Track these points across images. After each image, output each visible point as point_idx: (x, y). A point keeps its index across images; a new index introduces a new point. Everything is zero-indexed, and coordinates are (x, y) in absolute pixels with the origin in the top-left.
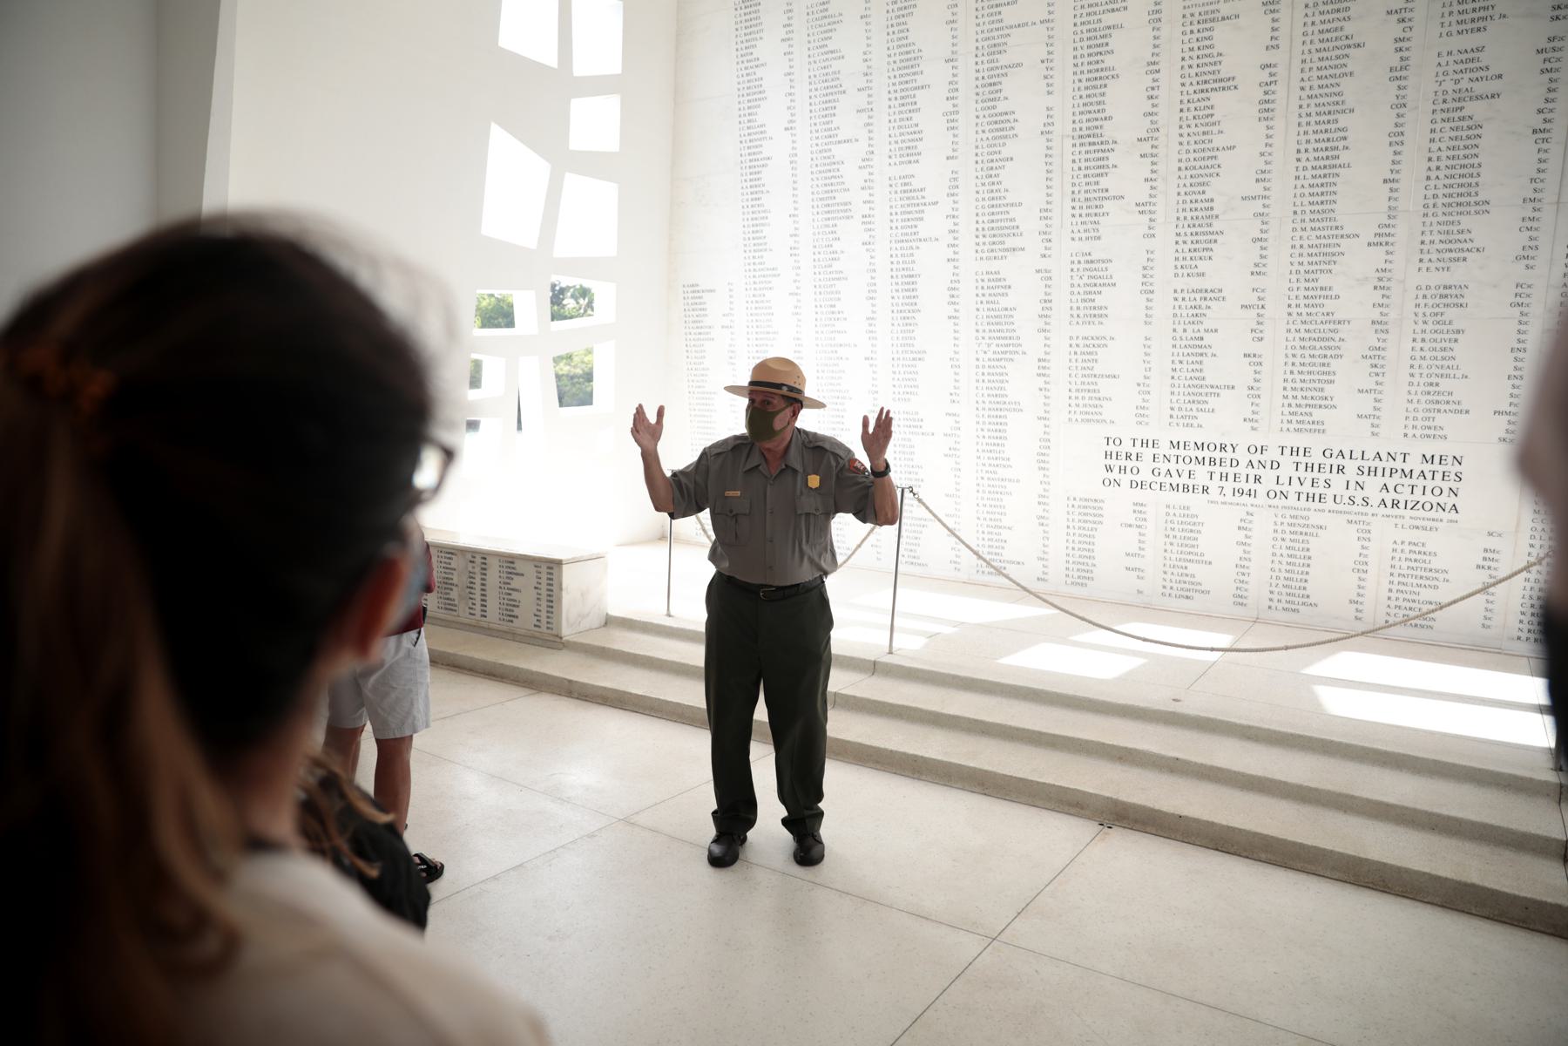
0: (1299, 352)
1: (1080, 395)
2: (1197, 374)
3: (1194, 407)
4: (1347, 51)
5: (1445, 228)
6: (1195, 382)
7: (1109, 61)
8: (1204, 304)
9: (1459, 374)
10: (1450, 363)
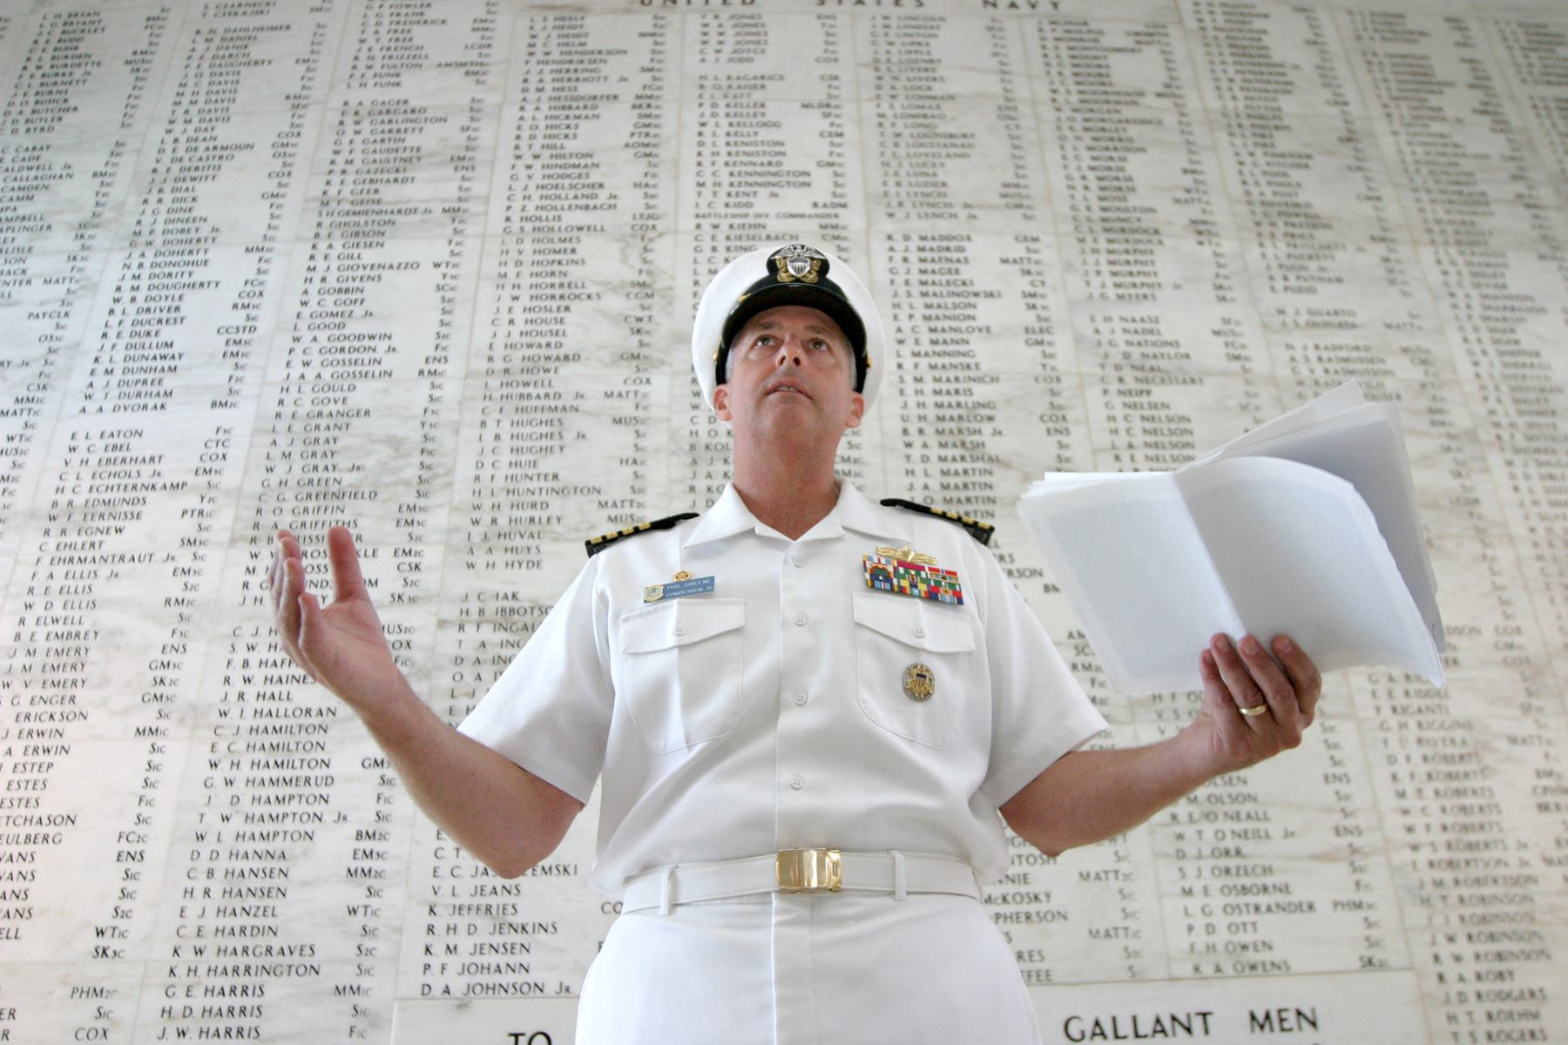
1: (462, 922)
4: (972, 300)
7: (575, 272)
10: (1248, 807)
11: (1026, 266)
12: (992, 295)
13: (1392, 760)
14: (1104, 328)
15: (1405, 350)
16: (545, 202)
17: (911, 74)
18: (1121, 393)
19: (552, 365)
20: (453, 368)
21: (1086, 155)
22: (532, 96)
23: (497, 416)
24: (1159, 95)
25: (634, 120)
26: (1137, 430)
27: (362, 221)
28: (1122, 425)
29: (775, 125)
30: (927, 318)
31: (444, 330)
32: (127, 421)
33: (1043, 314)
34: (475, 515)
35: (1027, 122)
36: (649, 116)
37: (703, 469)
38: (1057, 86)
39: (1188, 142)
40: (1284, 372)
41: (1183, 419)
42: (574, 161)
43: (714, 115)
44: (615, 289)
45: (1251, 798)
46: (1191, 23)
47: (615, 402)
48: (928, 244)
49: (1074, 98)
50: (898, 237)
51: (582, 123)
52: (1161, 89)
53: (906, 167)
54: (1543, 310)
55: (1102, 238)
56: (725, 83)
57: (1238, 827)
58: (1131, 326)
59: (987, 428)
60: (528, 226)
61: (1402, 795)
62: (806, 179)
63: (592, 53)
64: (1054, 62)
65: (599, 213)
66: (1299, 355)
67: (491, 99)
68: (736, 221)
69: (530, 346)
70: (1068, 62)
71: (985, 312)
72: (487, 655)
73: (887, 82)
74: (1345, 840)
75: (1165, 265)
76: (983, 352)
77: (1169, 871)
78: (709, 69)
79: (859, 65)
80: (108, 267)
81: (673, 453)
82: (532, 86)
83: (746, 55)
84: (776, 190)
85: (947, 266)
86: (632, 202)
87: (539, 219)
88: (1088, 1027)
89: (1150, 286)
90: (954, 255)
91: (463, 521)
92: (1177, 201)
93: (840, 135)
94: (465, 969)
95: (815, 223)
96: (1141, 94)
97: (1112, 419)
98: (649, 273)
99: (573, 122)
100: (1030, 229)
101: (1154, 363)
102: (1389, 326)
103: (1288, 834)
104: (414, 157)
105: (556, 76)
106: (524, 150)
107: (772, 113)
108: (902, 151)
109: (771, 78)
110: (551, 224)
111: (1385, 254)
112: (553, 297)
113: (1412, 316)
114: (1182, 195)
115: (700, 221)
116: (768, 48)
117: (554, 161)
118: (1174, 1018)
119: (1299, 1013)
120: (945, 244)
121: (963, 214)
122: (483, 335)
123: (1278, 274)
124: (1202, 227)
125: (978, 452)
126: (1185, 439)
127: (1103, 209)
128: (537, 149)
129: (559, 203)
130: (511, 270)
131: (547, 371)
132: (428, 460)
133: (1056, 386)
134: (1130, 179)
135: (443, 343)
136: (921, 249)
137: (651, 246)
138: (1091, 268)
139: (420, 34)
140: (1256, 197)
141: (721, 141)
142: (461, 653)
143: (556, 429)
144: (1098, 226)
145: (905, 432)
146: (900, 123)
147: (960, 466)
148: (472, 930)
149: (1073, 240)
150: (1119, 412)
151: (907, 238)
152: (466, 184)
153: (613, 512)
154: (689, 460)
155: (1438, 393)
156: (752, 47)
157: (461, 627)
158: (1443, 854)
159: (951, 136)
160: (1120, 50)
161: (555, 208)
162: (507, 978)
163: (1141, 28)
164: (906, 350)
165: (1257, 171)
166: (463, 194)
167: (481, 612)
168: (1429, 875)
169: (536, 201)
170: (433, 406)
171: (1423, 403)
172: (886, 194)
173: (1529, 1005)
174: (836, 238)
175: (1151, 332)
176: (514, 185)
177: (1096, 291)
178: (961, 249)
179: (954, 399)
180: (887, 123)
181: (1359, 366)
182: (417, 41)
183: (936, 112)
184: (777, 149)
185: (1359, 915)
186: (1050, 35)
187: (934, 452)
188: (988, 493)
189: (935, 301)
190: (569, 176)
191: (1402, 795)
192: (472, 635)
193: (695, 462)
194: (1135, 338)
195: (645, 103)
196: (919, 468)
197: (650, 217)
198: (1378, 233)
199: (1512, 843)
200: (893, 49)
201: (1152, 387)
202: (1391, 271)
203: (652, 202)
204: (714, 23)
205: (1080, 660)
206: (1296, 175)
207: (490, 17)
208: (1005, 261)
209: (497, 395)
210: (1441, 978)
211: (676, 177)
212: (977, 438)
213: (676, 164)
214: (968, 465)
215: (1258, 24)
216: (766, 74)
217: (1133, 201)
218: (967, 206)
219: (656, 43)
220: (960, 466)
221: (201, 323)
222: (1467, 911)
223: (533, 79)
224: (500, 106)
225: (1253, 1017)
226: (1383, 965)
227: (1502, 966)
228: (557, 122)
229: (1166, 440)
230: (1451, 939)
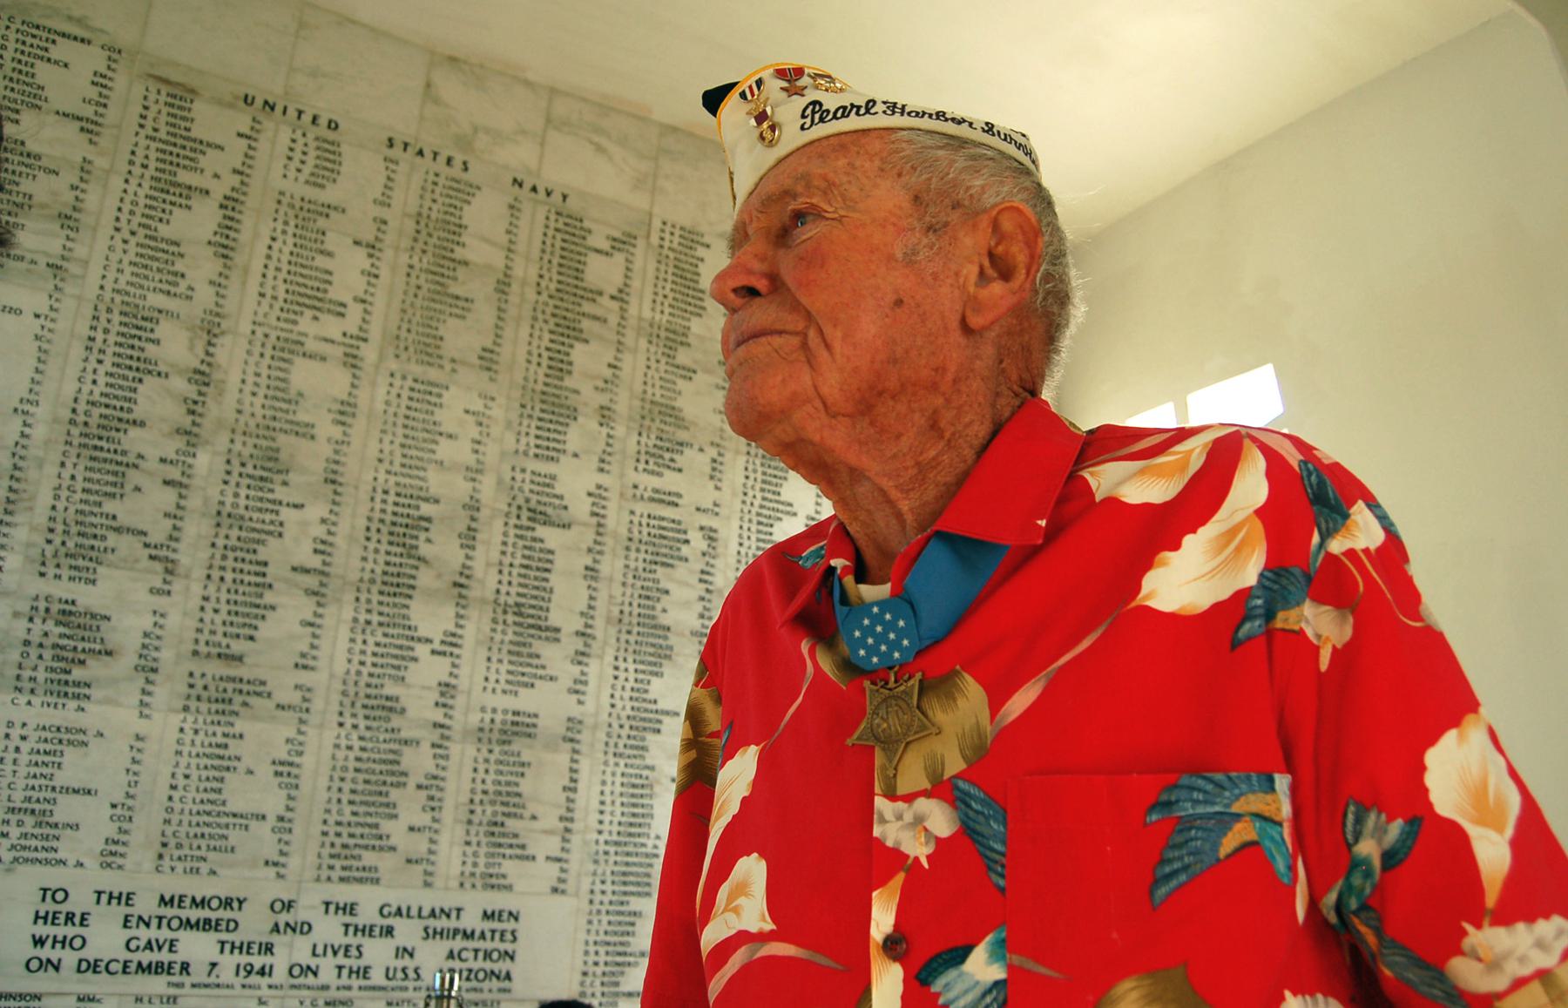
0: (350, 775)
1: (14, 818)
2: (213, 796)
3: (203, 843)
4: (438, 438)
5: (516, 649)
6: (208, 807)
8: (238, 699)
9: (527, 814)
10: (516, 800)
11: (481, 419)
12: (450, 436)
13: (604, 783)
14: (519, 476)
15: (702, 528)
16: (135, 279)
17: (442, 234)
18: (516, 526)
19: (123, 426)
21: (547, 336)
22: (137, 170)
23: (74, 460)
24: (613, 298)
25: (219, 219)
26: (519, 555)
28: (510, 549)
29: (330, 254)
30: (403, 446)
31: (38, 377)
33: (481, 457)
34: (50, 536)
35: (514, 299)
36: (232, 219)
37: (223, 531)
38: (544, 272)
39: (619, 342)
40: (624, 532)
41: (551, 552)
42: (163, 246)
43: (284, 232)
44: (180, 372)
45: (519, 795)
46: (655, 240)
47: (168, 467)
48: (418, 386)
49: (553, 286)
50: (398, 376)
51: (176, 210)
52: (615, 293)
53: (417, 318)
54: (795, 514)
55: (538, 406)
56: (298, 204)
57: (506, 810)
58: (537, 479)
59: (423, 536)
60: (118, 298)
61: (602, 803)
62: (342, 310)
63: (195, 140)
64: (549, 249)
65: (177, 300)
66: (636, 520)
67: (101, 163)
68: (283, 335)
69: (107, 406)
70: (558, 252)
71: (444, 449)
72: (48, 642)
73: (423, 237)
74: (562, 825)
75: (574, 438)
76: (435, 481)
77: (460, 831)
79: (406, 215)
81: (204, 515)
82: (139, 160)
83: (320, 181)
84: (318, 314)
85: (426, 407)
86: (205, 296)
87: (127, 293)
88: (394, 910)
89: (558, 451)
90: (433, 399)
91: (39, 539)
92: (597, 388)
93: (376, 276)
94: (13, 847)
95: (342, 349)
96: (600, 293)
97: (505, 543)
98: (209, 364)
99: (168, 207)
100: (492, 389)
101: (542, 508)
102: (698, 509)
103: (534, 818)
105: (161, 156)
106: (123, 224)
107: (331, 242)
108: (418, 302)
109: (336, 208)
110: (137, 301)
111: (715, 455)
112: (130, 368)
113: (716, 505)
114: (601, 384)
115: (257, 328)
116: (339, 179)
117: (147, 242)
118: (442, 910)
119: (511, 914)
120: (430, 389)
121: (448, 367)
122: (70, 388)
123: (643, 458)
124: (606, 413)
125: (413, 552)
126: (548, 566)
127: (546, 384)
128: (134, 226)
129: (146, 283)
130: (100, 336)
131: (118, 430)
132: (15, 485)
133: (476, 514)
134: (570, 363)
135: (36, 388)
136: (412, 389)
137: (214, 341)
138: (524, 429)
140: (649, 396)
141: (285, 258)
142: (29, 638)
143: (119, 480)
144: (538, 397)
145: (368, 529)
146: (423, 276)
147: (398, 560)
148: (20, 823)
149: (517, 405)
150: (511, 540)
151: (404, 378)
152: (69, 244)
153: (154, 552)
154: (214, 522)
155: (712, 561)
156: (327, 174)
157: (31, 620)
158: (615, 838)
159: (457, 298)
160: (598, 251)
161: (142, 287)
162: (42, 855)
163: (617, 235)
164: (382, 468)
165: (657, 376)
166: (66, 253)
167: (47, 610)
168: (602, 847)
169: (126, 277)
170: (24, 441)
171: (702, 566)
172: (398, 337)
173: (632, 919)
174: (354, 366)
175: (548, 485)
176: (111, 255)
177: (522, 448)
178: (439, 396)
179: (406, 511)
180: (414, 274)
181: (670, 534)
182: (39, 80)
183: (451, 274)
184: (327, 277)
185: (558, 865)
186: (552, 224)
187: (384, 547)
188: (412, 582)
189: (411, 433)
190: (157, 259)
191: (602, 803)
192: (38, 627)
193: (218, 525)
194: (536, 488)
195: (231, 204)
196: (371, 557)
197: (218, 315)
198: (717, 440)
199: (653, 836)
200: (435, 207)
201: (538, 526)
202: (714, 469)
203: (221, 301)
204: (301, 141)
205: (442, 700)
206: (681, 384)
207: (110, 74)
208: (467, 412)
209: (76, 442)
210: (591, 902)
211: (244, 283)
212: (414, 542)
213: (246, 270)
214: (404, 561)
215: (701, 252)
216: (333, 204)
217: (568, 382)
218: (453, 361)
219: (250, 147)
220: (398, 560)
222: (616, 869)
223: (140, 152)
224: (108, 172)
225: (485, 913)
226: (563, 892)
227: (625, 898)
228: (155, 204)
229: (534, 564)
230: (603, 882)
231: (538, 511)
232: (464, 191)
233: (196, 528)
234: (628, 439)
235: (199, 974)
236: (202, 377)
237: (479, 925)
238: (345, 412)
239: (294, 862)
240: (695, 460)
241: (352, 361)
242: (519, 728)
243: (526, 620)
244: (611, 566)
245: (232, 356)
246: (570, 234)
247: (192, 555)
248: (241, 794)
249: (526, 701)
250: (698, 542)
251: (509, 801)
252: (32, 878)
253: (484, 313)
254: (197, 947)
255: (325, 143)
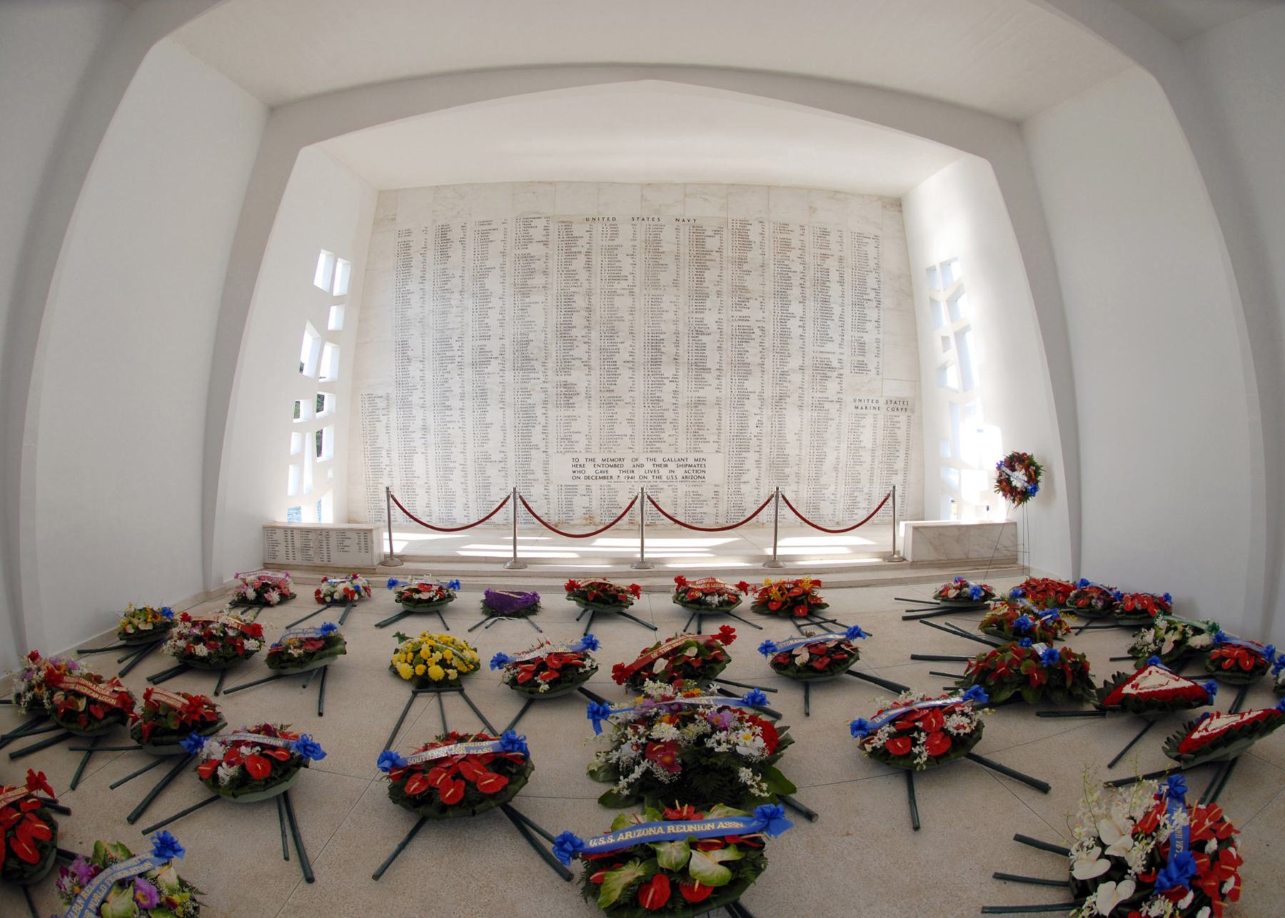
20: (549, 330)
27: (524, 290)
32: (483, 342)
71: (665, 316)
75: (708, 303)
76: (663, 327)
78: (604, 243)
80: (469, 303)
104: (534, 271)
139: (531, 231)
221: (493, 318)
231: (699, 331)
232: (659, 228)
233: (595, 354)
234: (728, 301)
235: (615, 479)
236: (589, 309)
237: (694, 463)
238: (632, 310)
239: (636, 448)
240: (754, 304)
241: (632, 294)
242: (700, 402)
243: (699, 367)
244: (727, 345)
245: (596, 300)
246: (699, 234)
247: (595, 363)
248: (619, 430)
249: (701, 393)
250: (758, 332)
251: (700, 425)
252: (570, 456)
253: (672, 267)
254: (613, 472)
255: (612, 224)
